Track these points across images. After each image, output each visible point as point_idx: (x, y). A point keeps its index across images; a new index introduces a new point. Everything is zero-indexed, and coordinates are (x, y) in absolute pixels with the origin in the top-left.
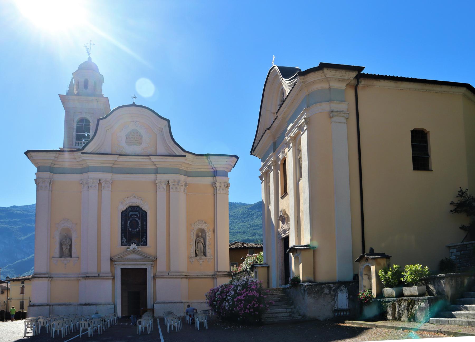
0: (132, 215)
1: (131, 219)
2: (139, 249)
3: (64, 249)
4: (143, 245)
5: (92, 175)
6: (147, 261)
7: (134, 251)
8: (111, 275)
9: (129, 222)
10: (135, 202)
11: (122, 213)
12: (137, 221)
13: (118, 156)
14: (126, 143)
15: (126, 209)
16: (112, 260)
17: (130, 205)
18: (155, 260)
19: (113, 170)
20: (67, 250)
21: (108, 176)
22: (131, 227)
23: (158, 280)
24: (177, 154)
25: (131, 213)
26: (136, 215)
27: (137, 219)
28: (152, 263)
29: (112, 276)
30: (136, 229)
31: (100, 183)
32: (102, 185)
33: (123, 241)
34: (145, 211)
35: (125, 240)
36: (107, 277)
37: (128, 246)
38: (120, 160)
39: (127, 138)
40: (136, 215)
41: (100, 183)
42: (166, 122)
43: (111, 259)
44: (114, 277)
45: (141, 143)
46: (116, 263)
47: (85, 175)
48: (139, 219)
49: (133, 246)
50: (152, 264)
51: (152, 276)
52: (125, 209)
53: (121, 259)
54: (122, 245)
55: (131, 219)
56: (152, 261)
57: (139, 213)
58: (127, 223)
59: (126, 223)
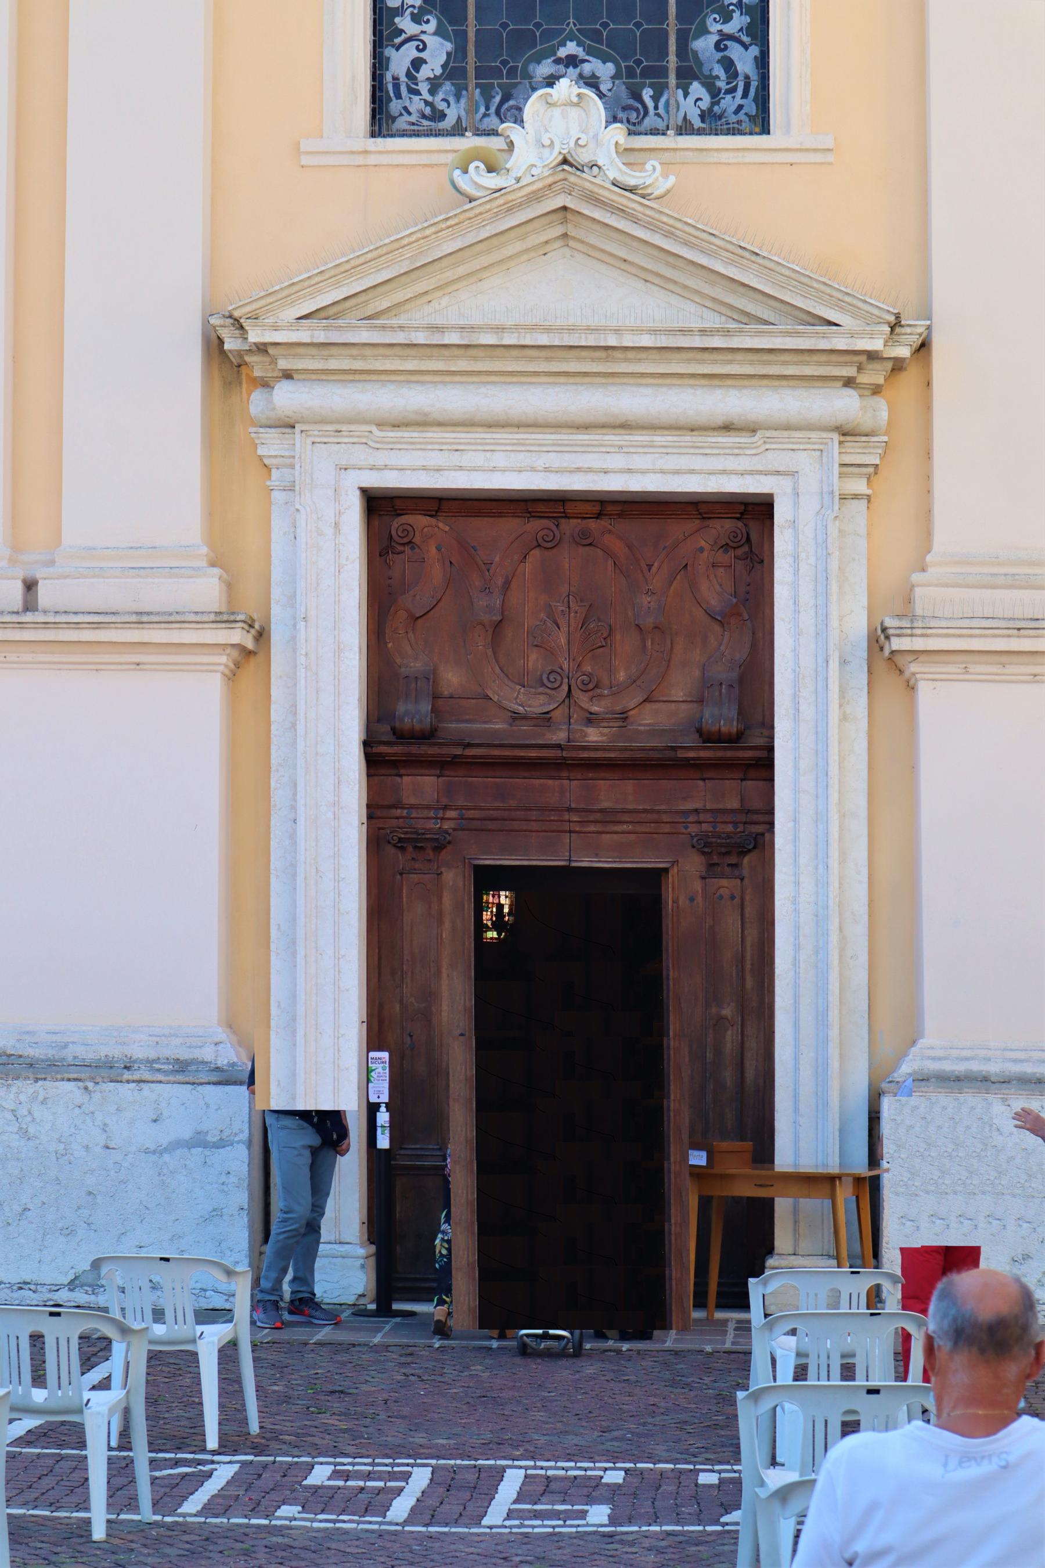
2: (653, 176)
4: (712, 122)
6: (768, 368)
7: (570, 213)
8: (206, 590)
16: (231, 363)
18: (908, 361)
23: (937, 699)
28: (845, 405)
29: (224, 619)
33: (399, 61)
35: (437, 53)
36: (142, 619)
37: (469, 142)
43: (214, 348)
44: (262, 636)
46: (287, 398)
49: (563, 117)
50: (846, 432)
51: (858, 626)
53: (362, 327)
54: (381, 120)
56: (855, 369)
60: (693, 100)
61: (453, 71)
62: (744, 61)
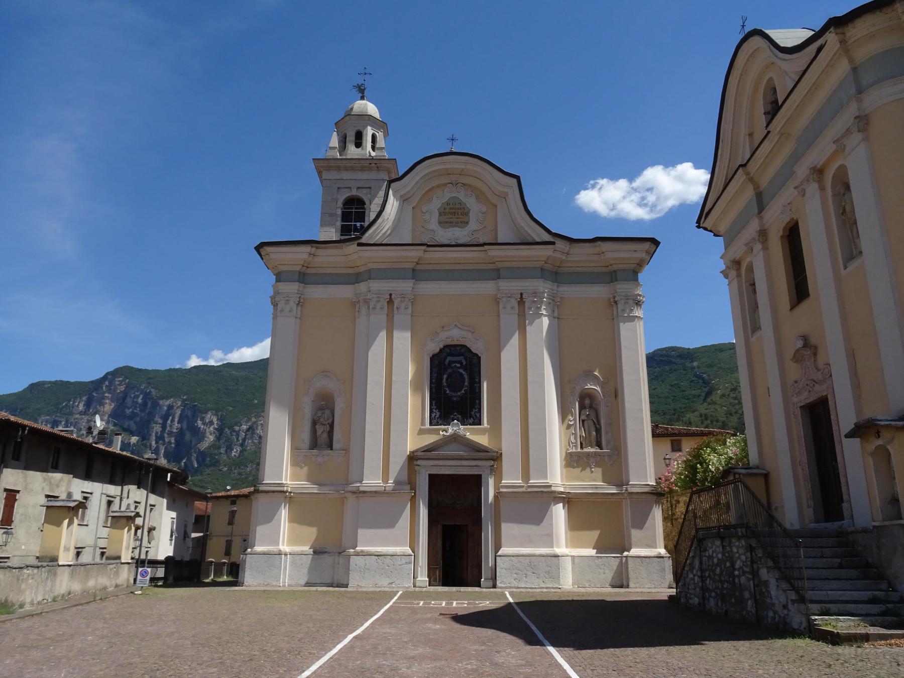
0: (451, 362)
1: (449, 371)
3: (319, 433)
5: (375, 285)
9: (445, 376)
10: (456, 336)
11: (432, 359)
12: (461, 374)
13: (424, 248)
14: (440, 223)
15: (441, 350)
17: (449, 342)
19: (416, 274)
20: (325, 435)
21: (405, 286)
22: (448, 386)
24: (538, 240)
25: (449, 358)
26: (460, 362)
27: (461, 371)
30: (460, 391)
31: (390, 302)
32: (396, 305)
33: (433, 415)
34: (477, 355)
35: (438, 414)
38: (429, 255)
39: (440, 214)
40: (460, 362)
41: (390, 302)
42: (515, 181)
45: (467, 223)
47: (363, 287)
48: (465, 370)
52: (437, 350)
55: (449, 371)
57: (466, 358)
58: (442, 379)
59: (439, 379)
60: (471, 421)
61: (440, 417)
62: (478, 415)
